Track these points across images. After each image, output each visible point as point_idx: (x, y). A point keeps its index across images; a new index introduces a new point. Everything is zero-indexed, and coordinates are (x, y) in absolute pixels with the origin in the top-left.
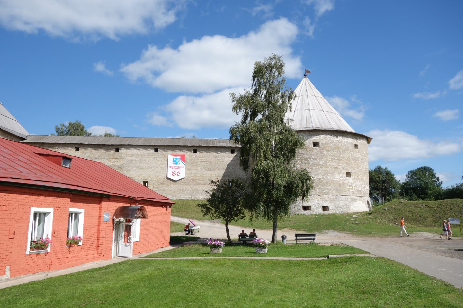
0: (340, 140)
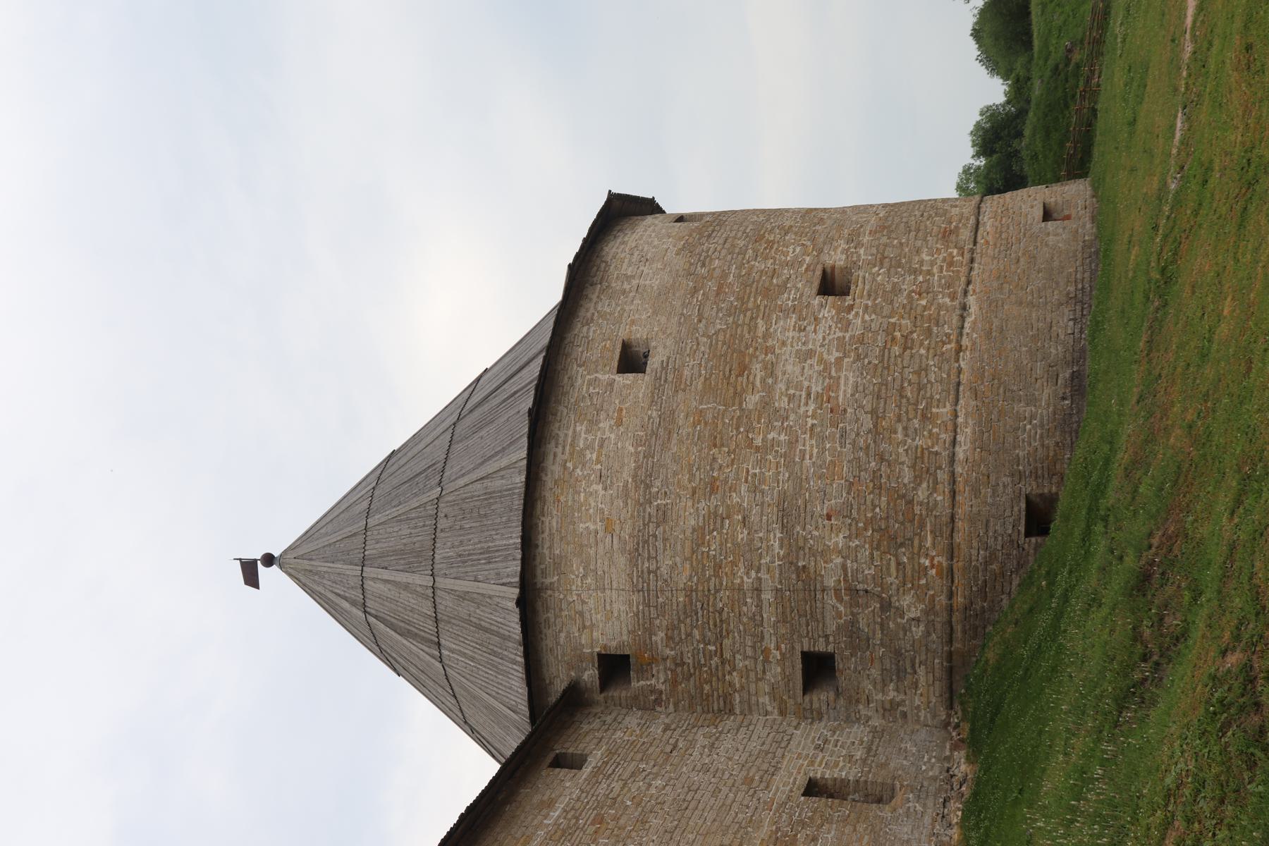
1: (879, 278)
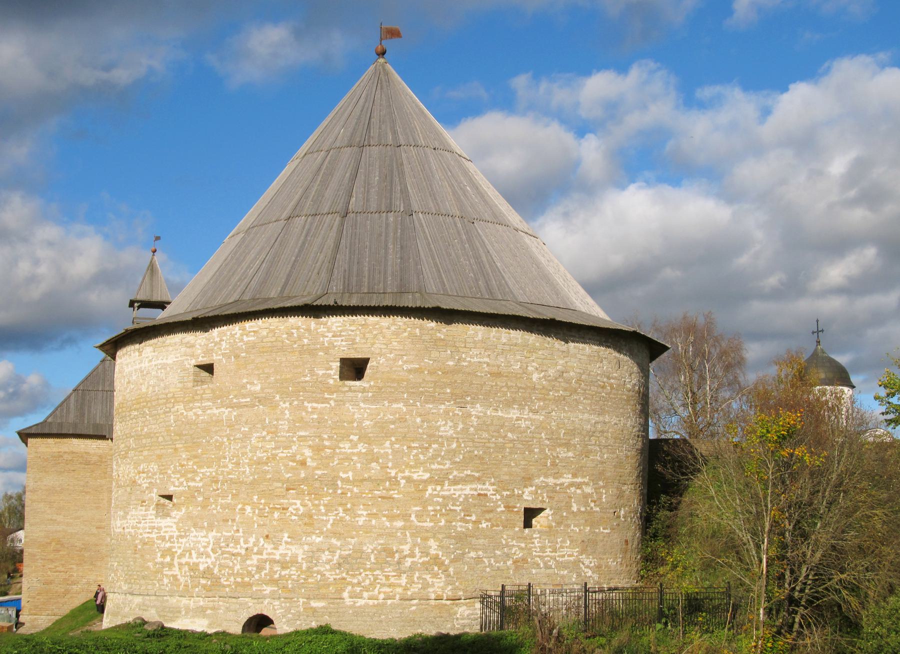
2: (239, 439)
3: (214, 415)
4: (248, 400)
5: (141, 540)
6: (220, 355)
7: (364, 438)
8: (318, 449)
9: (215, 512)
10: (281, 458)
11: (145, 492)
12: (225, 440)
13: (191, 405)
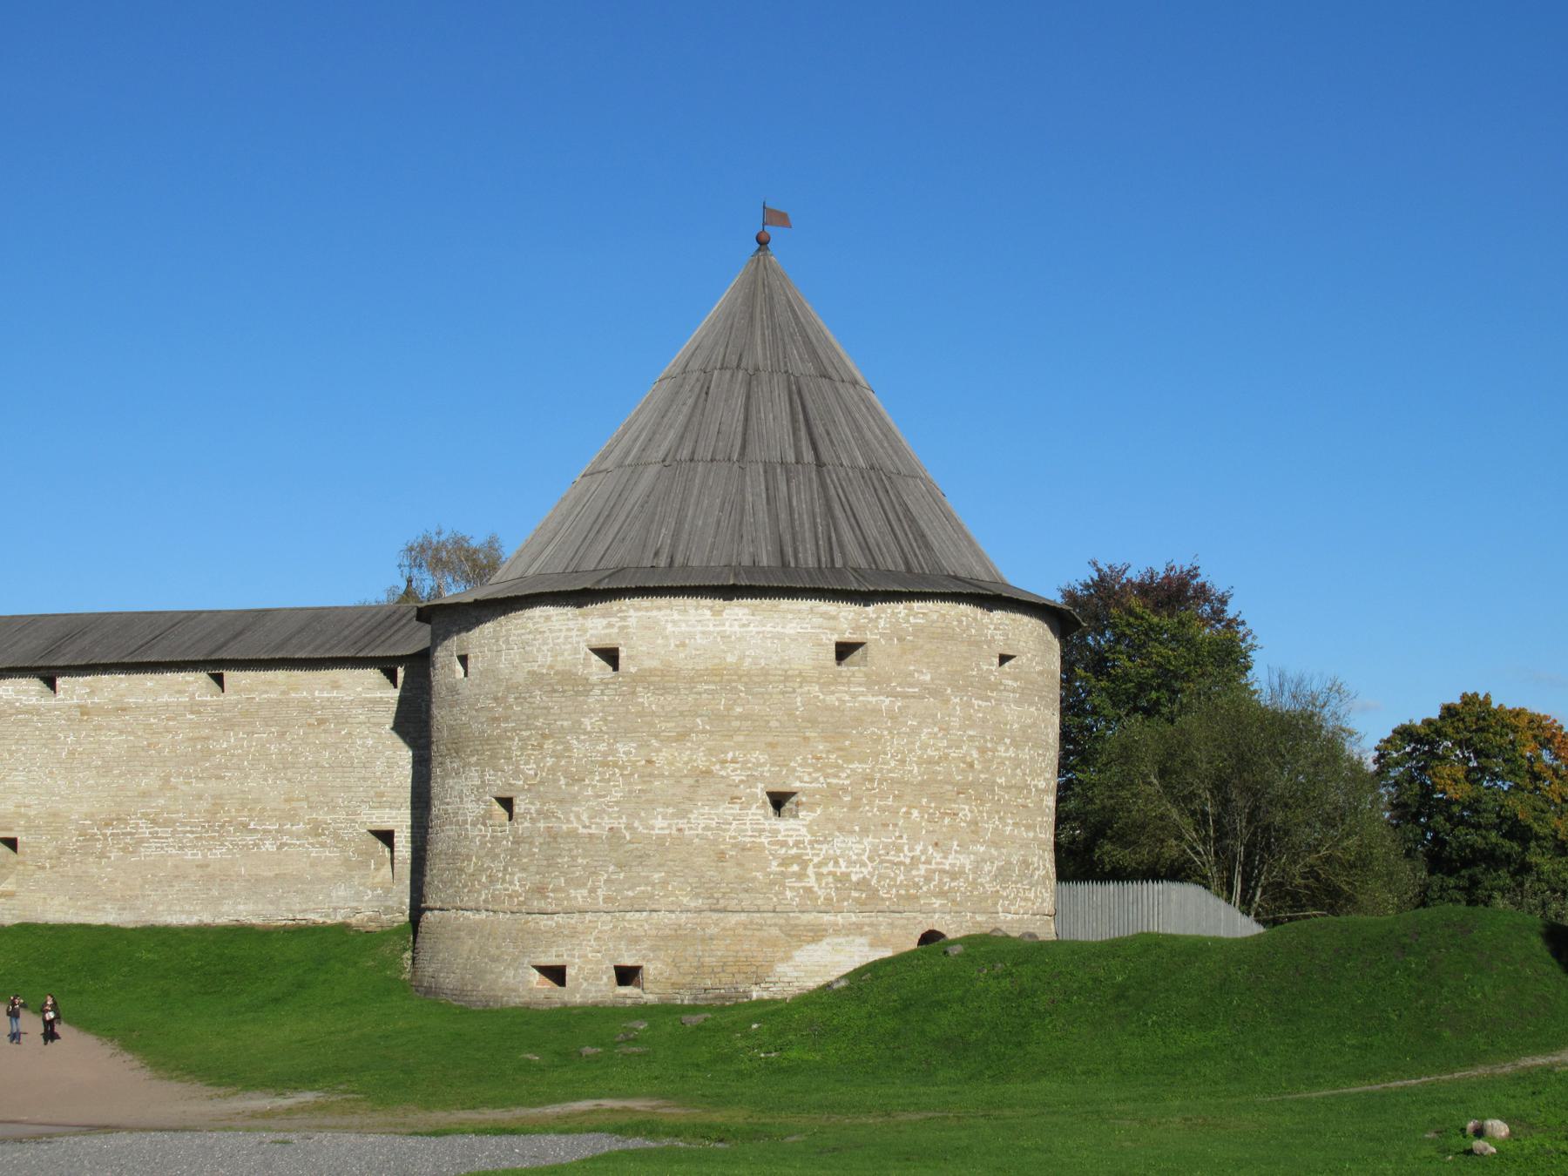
0: (736, 628)
1: (505, 842)
2: (905, 733)
3: (869, 702)
4: (917, 690)
5: (734, 846)
6: (876, 634)
7: (1015, 744)
8: (982, 751)
9: (870, 814)
10: (954, 758)
11: (737, 786)
12: (886, 733)
13: (833, 688)
